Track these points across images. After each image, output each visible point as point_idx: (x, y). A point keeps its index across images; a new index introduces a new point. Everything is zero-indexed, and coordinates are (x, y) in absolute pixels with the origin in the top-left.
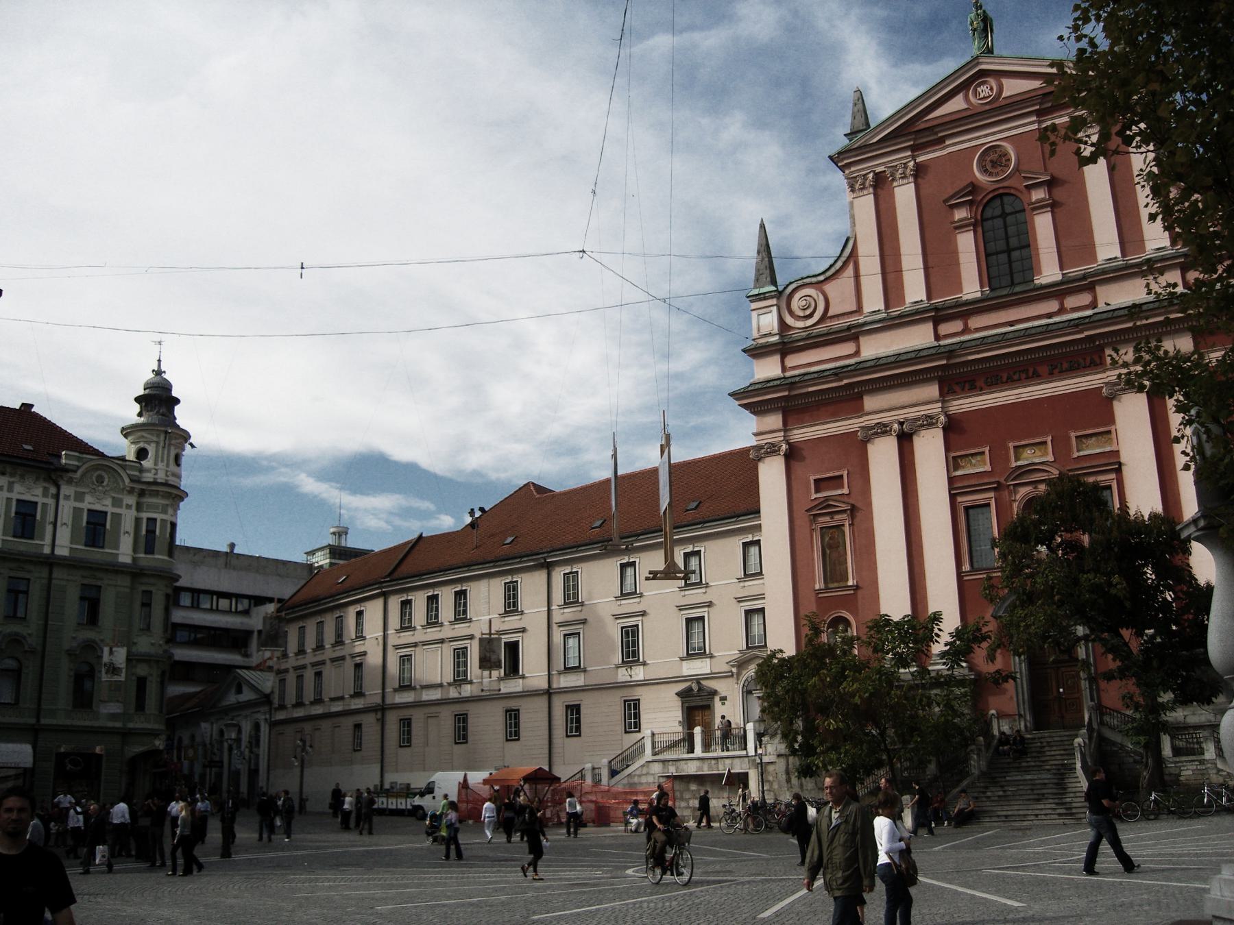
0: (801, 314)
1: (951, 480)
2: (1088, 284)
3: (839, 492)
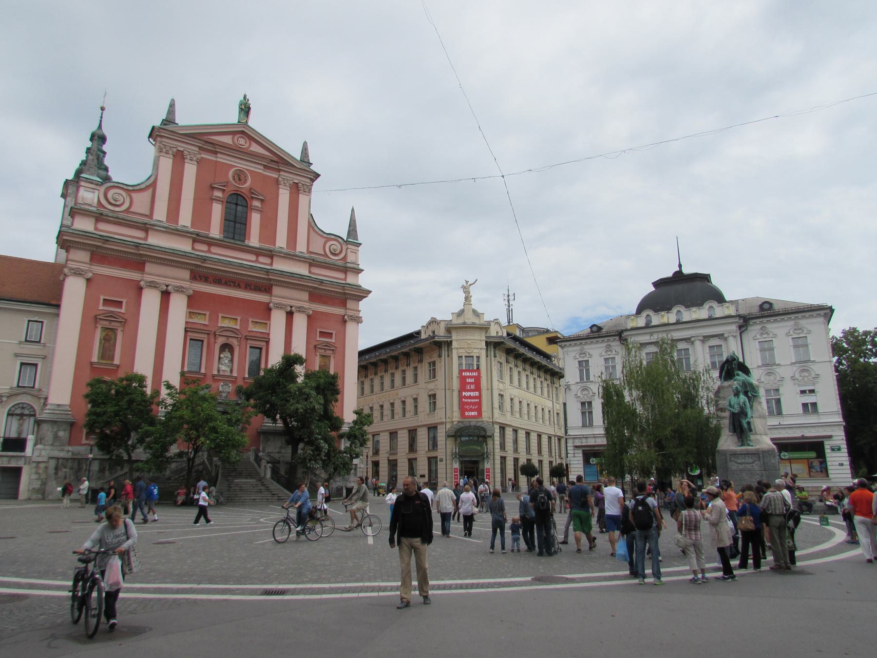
0: (113, 202)
1: (186, 323)
2: (271, 255)
3: (119, 310)
